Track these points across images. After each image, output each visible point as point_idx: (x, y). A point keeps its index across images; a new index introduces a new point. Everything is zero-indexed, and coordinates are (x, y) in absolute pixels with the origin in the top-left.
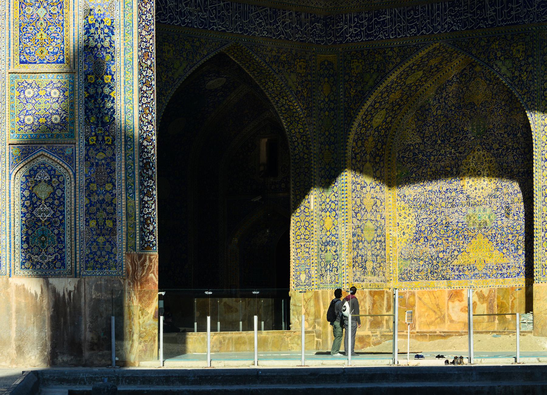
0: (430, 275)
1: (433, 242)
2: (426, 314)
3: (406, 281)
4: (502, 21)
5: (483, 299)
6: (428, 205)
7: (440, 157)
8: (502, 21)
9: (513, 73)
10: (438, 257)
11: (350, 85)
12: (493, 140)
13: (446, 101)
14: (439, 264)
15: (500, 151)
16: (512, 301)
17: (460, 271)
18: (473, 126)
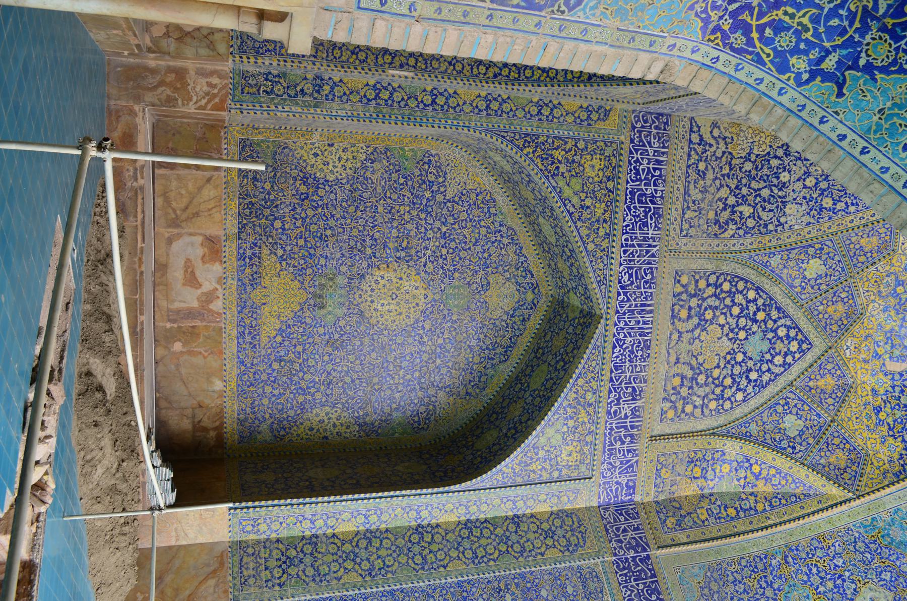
0: (247, 201)
1: (299, 210)
2: (183, 192)
3: (240, 154)
4: (611, 429)
5: (206, 301)
6: (356, 204)
7: (423, 230)
8: (611, 429)
9: (543, 449)
10: (276, 219)
11: (570, 150)
12: (436, 319)
13: (496, 244)
14: (264, 220)
15: (421, 332)
16: (200, 353)
17: (251, 259)
18: (458, 287)
